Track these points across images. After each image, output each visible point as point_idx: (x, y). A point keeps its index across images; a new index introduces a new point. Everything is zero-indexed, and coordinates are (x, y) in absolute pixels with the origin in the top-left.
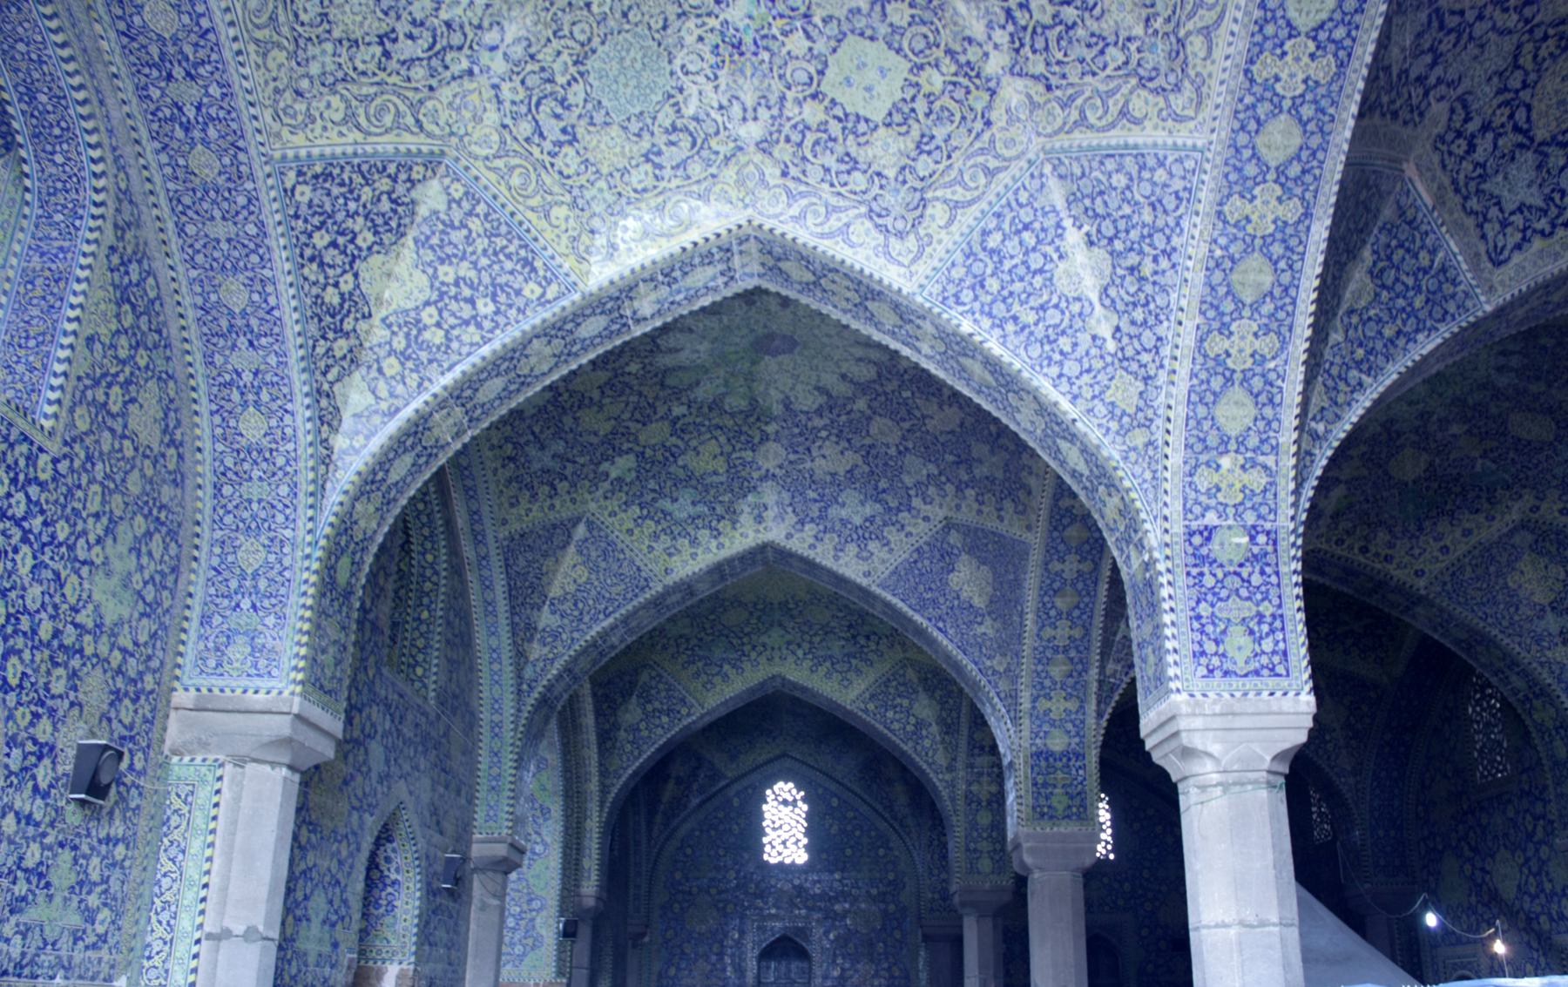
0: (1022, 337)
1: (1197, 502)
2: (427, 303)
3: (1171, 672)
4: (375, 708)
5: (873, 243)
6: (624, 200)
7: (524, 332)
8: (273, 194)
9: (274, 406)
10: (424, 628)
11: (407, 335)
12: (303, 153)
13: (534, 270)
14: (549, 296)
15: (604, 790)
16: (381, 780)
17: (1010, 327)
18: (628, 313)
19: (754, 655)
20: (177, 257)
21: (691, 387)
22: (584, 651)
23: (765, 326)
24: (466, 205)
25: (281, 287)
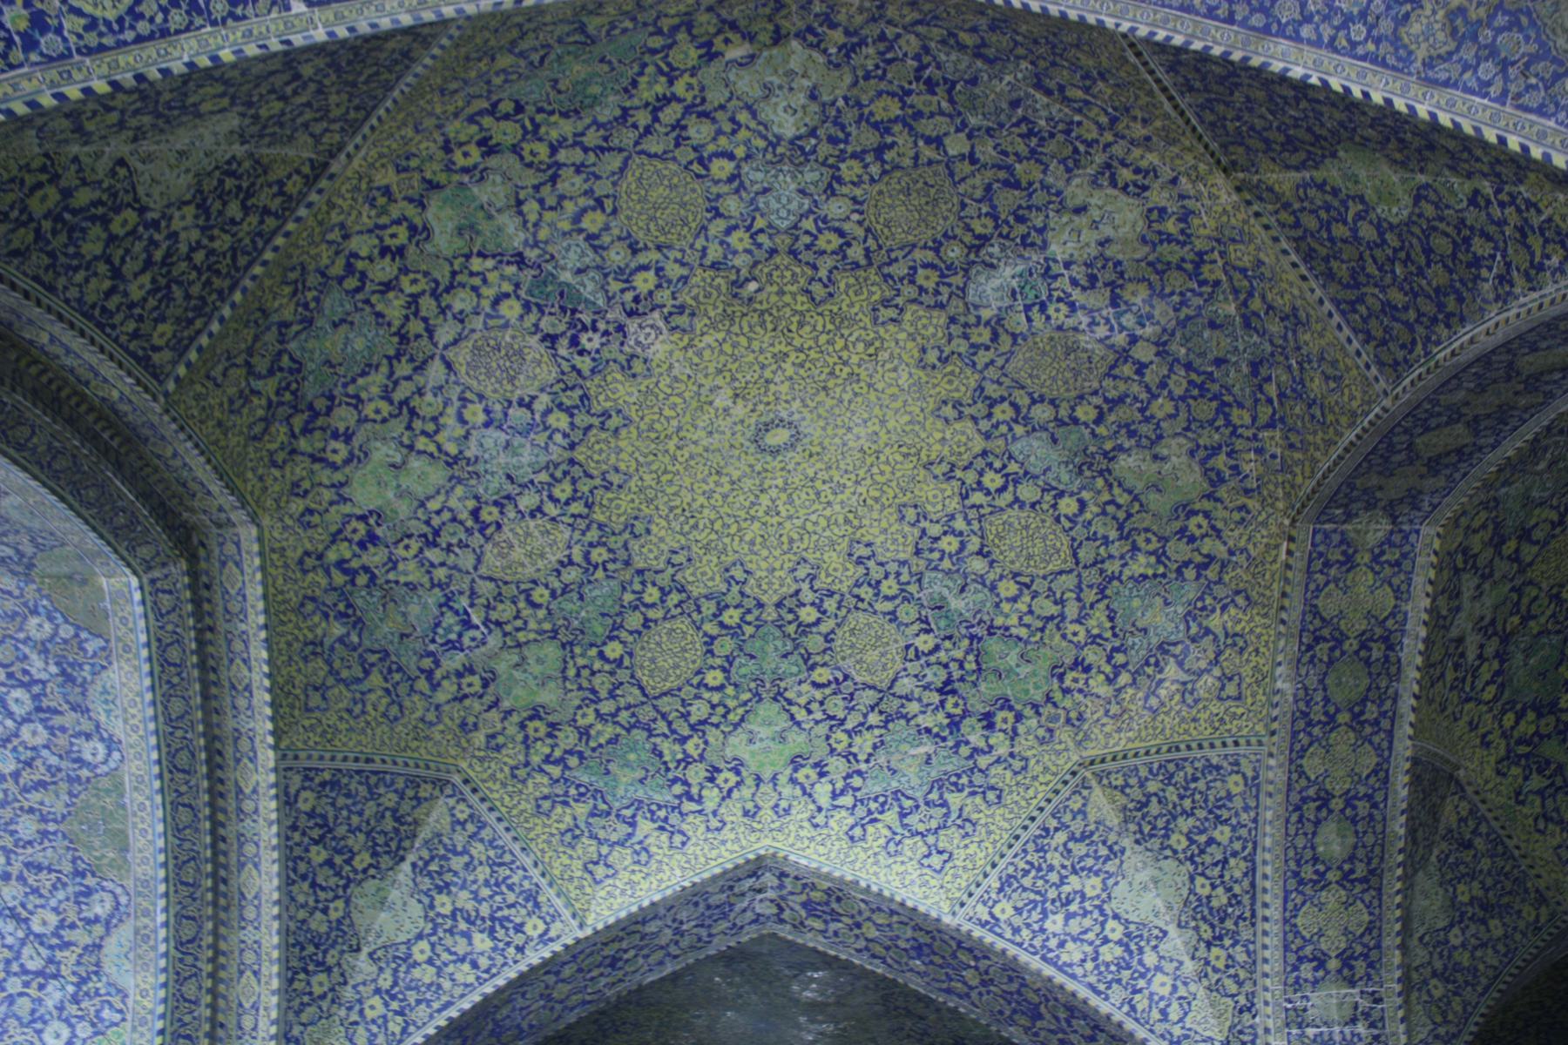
19: (711, 796)
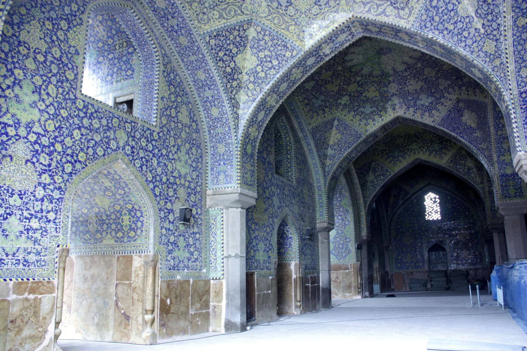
0: (450, 35)
1: (522, 81)
2: (258, 65)
3: (517, 144)
4: (273, 187)
5: (394, 14)
6: (311, 19)
7: (288, 68)
8: (203, 45)
9: (219, 105)
10: (289, 161)
11: (254, 76)
12: (209, 30)
13: (287, 48)
14: (294, 55)
15: (365, 202)
16: (279, 208)
17: (445, 32)
18: (322, 54)
19: (408, 153)
20: (184, 68)
21: (360, 71)
22: (344, 160)
23: (379, 46)
24: (263, 33)
25: (213, 71)
